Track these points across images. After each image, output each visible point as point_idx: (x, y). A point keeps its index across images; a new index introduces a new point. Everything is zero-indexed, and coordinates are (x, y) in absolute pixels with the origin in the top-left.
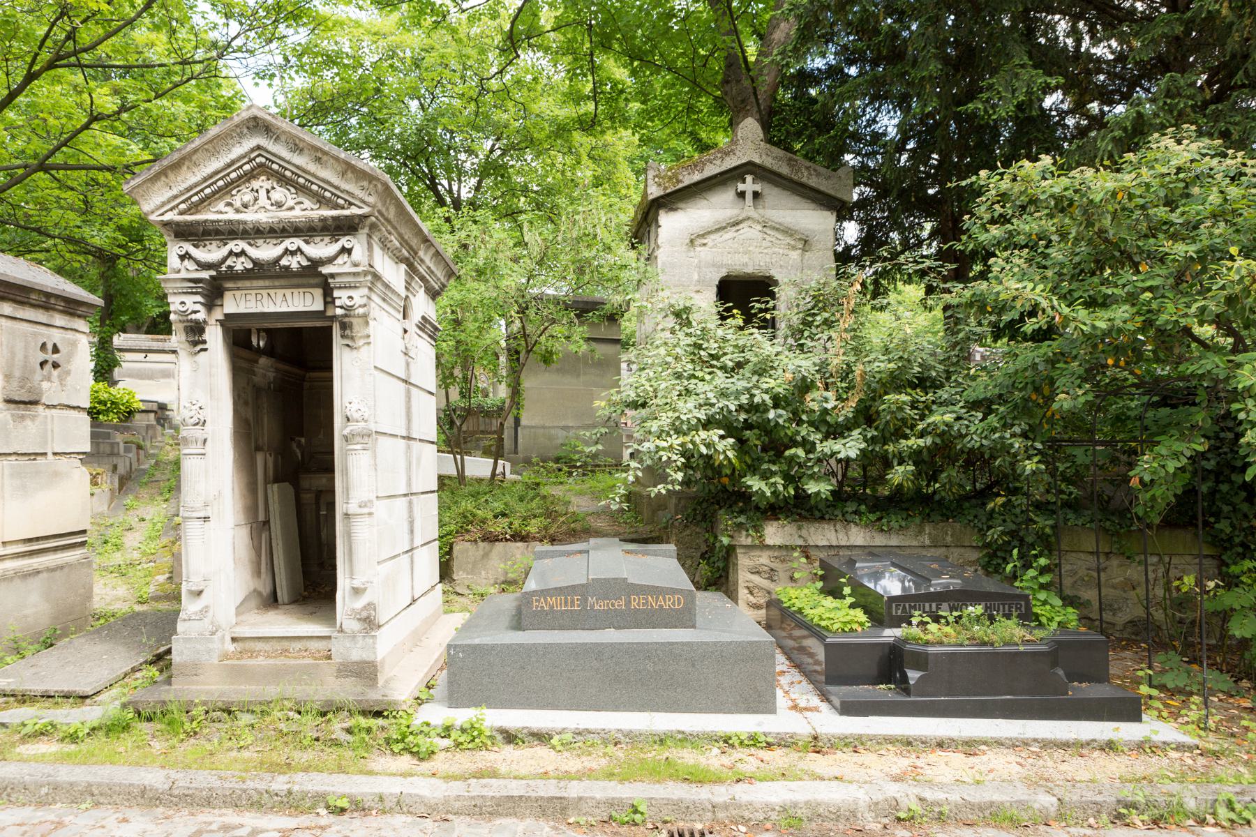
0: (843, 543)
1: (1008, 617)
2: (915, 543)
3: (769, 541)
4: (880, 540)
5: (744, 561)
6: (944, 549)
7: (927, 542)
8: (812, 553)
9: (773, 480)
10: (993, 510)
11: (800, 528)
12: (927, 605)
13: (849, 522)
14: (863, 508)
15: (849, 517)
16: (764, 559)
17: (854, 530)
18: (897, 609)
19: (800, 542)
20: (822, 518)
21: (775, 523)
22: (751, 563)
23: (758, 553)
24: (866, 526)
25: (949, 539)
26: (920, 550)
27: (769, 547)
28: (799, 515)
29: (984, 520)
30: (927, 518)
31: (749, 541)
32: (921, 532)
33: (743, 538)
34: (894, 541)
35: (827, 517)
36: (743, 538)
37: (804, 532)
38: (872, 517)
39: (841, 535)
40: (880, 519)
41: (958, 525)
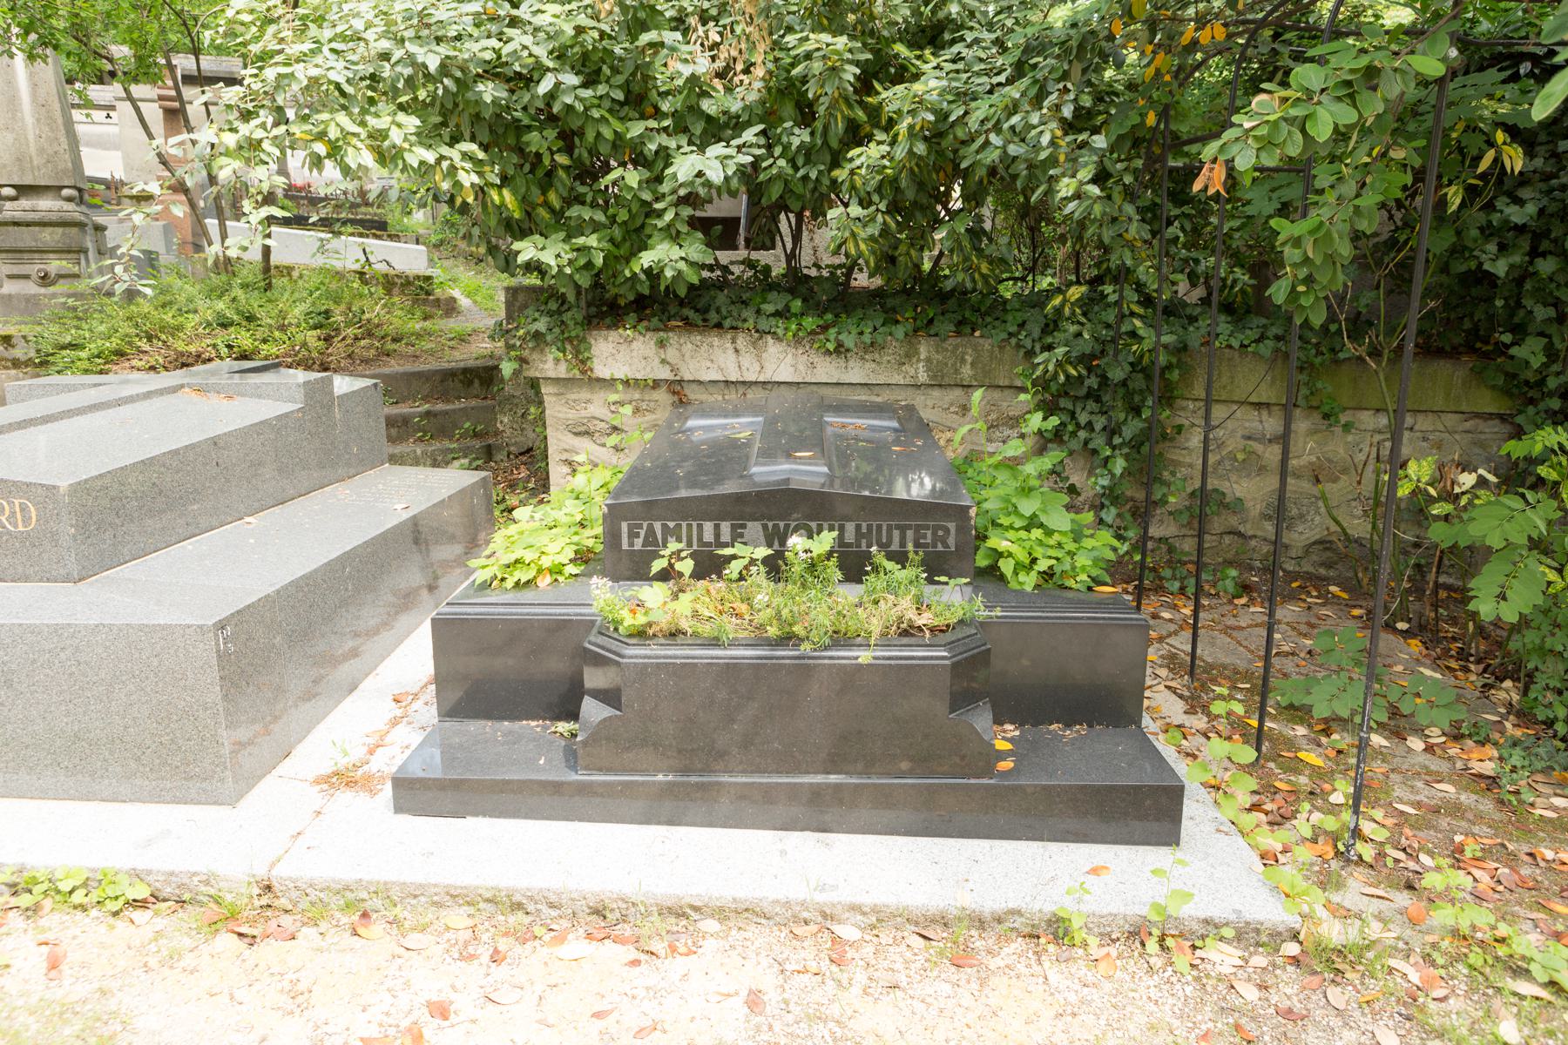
0: (751, 377)
1: (901, 558)
2: (897, 379)
3: (601, 370)
4: (827, 370)
5: (556, 409)
6: (958, 392)
7: (923, 377)
8: (693, 393)
9: (581, 241)
10: (1058, 311)
11: (661, 344)
12: (708, 527)
13: (762, 333)
14: (797, 305)
15: (764, 324)
16: (597, 406)
17: (773, 348)
18: (633, 535)
19: (664, 374)
20: (719, 326)
21: (613, 335)
22: (572, 415)
23: (584, 394)
24: (798, 341)
25: (967, 371)
26: (910, 391)
27: (610, 383)
28: (685, 319)
29: (1036, 333)
30: (925, 327)
31: (562, 371)
32: (911, 355)
33: (550, 365)
34: (856, 372)
35: (727, 323)
36: (550, 365)
37: (671, 354)
38: (810, 322)
39: (748, 360)
40: (825, 328)
41: (986, 344)
